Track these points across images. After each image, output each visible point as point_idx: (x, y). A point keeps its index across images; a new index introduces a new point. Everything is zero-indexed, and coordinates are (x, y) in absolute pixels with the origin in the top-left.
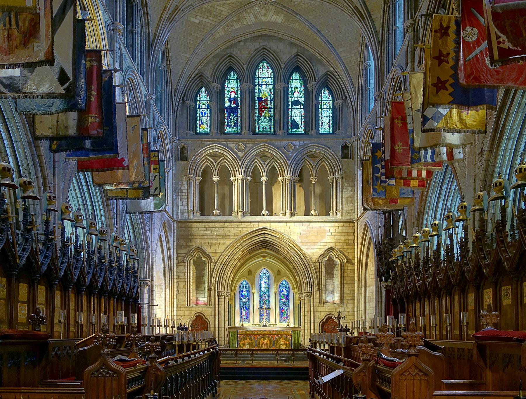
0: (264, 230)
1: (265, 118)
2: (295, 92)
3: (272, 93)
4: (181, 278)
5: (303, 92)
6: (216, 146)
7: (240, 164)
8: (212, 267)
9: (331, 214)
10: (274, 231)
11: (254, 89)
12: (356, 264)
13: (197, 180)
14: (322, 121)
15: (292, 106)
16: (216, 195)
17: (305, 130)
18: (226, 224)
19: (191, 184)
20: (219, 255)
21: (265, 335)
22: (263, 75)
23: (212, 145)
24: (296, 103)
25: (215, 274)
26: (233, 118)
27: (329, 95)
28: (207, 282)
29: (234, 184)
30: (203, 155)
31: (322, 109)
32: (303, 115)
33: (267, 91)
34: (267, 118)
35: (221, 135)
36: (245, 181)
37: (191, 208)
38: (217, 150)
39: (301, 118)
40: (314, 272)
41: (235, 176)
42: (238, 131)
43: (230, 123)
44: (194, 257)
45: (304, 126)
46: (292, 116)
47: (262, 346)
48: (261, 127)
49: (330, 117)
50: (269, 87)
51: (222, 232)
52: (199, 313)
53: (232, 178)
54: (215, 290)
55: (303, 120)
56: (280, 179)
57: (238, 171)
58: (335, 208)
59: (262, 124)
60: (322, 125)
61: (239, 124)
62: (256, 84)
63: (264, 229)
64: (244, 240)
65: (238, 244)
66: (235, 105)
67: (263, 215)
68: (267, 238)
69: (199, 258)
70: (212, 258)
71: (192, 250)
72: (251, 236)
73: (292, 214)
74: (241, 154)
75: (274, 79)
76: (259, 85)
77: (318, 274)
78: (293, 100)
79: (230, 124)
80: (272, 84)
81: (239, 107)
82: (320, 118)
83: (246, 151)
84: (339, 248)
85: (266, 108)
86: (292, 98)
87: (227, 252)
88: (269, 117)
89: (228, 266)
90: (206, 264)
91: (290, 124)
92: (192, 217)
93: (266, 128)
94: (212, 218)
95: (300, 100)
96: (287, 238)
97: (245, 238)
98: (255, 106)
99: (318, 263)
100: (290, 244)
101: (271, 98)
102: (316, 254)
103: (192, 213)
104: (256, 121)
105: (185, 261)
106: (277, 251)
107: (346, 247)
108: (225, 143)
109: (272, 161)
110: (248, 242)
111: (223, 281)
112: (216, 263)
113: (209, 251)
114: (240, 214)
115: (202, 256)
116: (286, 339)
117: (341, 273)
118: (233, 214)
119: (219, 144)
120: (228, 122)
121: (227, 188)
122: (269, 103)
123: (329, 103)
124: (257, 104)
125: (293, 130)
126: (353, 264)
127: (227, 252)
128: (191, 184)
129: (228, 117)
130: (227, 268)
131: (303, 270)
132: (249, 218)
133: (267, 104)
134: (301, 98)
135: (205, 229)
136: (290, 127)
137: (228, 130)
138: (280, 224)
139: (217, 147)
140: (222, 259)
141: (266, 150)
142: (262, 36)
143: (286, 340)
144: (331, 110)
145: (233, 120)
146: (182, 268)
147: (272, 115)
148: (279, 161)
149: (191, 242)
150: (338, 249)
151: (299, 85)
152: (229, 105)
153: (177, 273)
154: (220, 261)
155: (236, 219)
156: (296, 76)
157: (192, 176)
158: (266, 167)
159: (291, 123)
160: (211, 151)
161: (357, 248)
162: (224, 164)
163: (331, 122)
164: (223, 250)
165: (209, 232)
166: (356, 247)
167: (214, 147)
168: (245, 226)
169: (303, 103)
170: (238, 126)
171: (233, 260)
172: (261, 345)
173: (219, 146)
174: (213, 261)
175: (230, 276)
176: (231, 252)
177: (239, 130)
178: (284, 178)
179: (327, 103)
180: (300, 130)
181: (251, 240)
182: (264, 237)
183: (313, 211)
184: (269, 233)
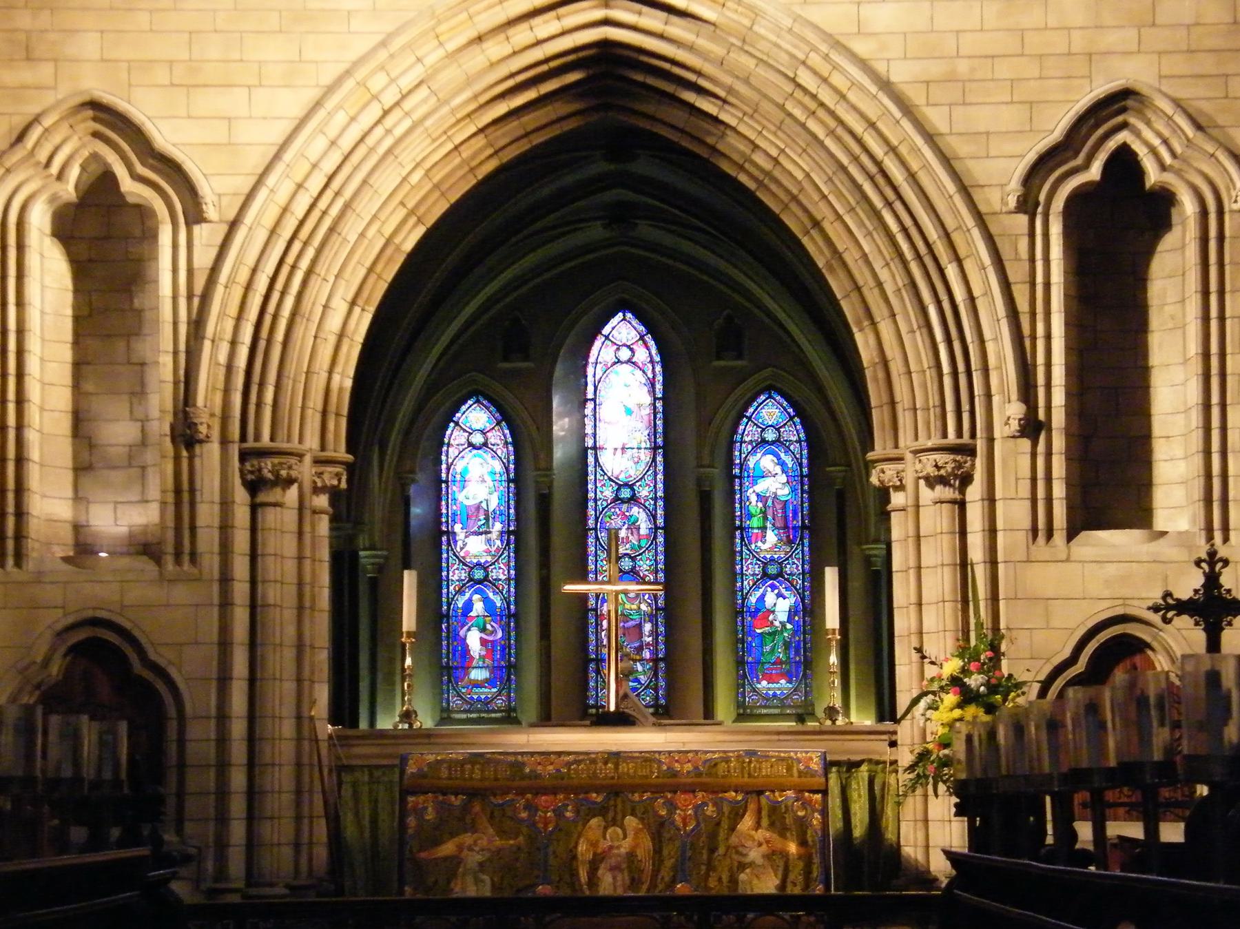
8: (203, 259)
20: (255, 161)
21: (615, 791)
40: (988, 292)
44: (60, 176)
47: (593, 880)
52: (95, 622)
54: (225, 442)
65: (406, 82)
70: (205, 189)
71: (36, 120)
77: (1023, 305)
84: (1183, 92)
87: (321, 143)
89: (328, 253)
90: (151, 236)
96: (778, 29)
100: (805, 78)
111: (291, 369)
112: (234, 225)
115: (120, 171)
116: (777, 819)
117: (1206, 293)
130: (321, 269)
140: (282, 197)
143: (783, 832)
149: (29, 57)
150: (1178, 103)
154: (262, 213)
164: (284, 128)
171: (367, 207)
172: (583, 875)
174: (211, 212)
175: (341, 336)
176: (346, 143)
182: (606, 22)
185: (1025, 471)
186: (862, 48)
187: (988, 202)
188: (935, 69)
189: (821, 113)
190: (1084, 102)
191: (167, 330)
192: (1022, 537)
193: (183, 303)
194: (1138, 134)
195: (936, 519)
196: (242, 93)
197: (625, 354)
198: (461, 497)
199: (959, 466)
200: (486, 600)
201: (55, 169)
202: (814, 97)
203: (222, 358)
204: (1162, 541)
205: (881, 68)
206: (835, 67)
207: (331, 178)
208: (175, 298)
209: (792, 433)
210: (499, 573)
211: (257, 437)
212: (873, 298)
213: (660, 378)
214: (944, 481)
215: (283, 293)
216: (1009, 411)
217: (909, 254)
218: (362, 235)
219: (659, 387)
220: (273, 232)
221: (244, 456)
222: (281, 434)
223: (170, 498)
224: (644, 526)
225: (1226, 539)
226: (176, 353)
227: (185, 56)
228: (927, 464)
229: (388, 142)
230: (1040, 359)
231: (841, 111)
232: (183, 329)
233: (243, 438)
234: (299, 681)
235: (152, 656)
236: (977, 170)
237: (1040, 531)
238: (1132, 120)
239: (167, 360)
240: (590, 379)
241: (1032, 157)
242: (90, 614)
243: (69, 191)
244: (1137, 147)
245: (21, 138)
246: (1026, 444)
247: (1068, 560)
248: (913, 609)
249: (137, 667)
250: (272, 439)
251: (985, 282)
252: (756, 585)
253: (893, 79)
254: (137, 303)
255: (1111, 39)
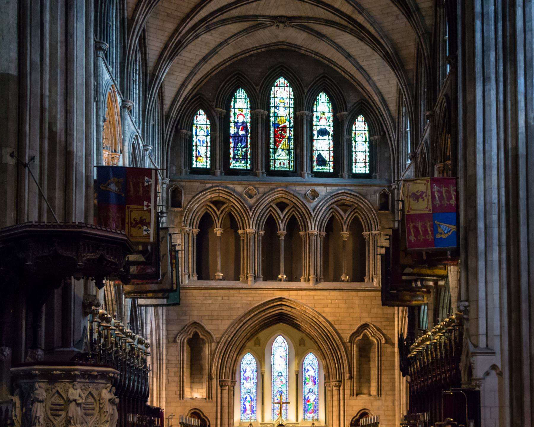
0: (281, 301)
1: (283, 150)
2: (321, 118)
3: (292, 119)
4: (173, 362)
5: (332, 119)
6: (219, 189)
7: (251, 214)
8: (213, 348)
9: (366, 280)
10: (294, 302)
11: (269, 112)
12: (396, 345)
13: (193, 233)
14: (356, 156)
15: (318, 137)
16: (219, 253)
17: (334, 168)
18: (232, 291)
19: (186, 237)
20: (222, 332)
22: (281, 94)
23: (214, 189)
24: (323, 132)
25: (216, 358)
26: (240, 149)
27: (365, 124)
28: (207, 367)
29: (242, 238)
30: (203, 201)
31: (356, 142)
32: (332, 149)
33: (285, 115)
34: (285, 151)
35: (225, 175)
36: (256, 235)
37: (186, 271)
38: (221, 195)
39: (329, 153)
41: (244, 229)
42: (247, 167)
43: (237, 155)
45: (334, 162)
46: (318, 149)
48: (277, 162)
49: (366, 152)
50: (288, 110)
51: (227, 302)
53: (240, 232)
54: (217, 379)
55: (332, 154)
56: (302, 233)
57: (247, 223)
58: (371, 273)
59: (279, 158)
60: (356, 163)
61: (249, 157)
62: (271, 105)
63: (281, 299)
64: (255, 313)
66: (243, 132)
67: (280, 280)
68: (286, 310)
69: (196, 335)
70: (214, 336)
71: (186, 325)
72: (264, 308)
73: (317, 281)
74: (251, 201)
75: (295, 100)
76: (276, 107)
77: (350, 358)
78: (319, 128)
79: (237, 157)
80: (293, 106)
81: (249, 135)
82: (354, 153)
83: (258, 196)
85: (284, 137)
86: (317, 125)
87: (233, 329)
88: (288, 150)
90: (205, 343)
91: (315, 159)
92: (187, 282)
93: (284, 164)
94: (213, 283)
95: (327, 128)
96: (310, 311)
97: (256, 311)
98: (269, 134)
99: (350, 344)
101: (291, 125)
102: (347, 332)
103: (187, 276)
104: (271, 155)
105: (177, 341)
106: (297, 327)
107: (384, 323)
108: (231, 186)
109: (292, 210)
110: (260, 316)
112: (218, 343)
113: (208, 328)
114: (250, 279)
115: (200, 334)
117: (378, 357)
118: (241, 279)
119: (223, 187)
120: (234, 155)
121: (232, 241)
122: (288, 131)
123: (365, 134)
124: (272, 132)
125: (319, 167)
126: (393, 345)
127: (233, 329)
128: (186, 237)
129: (234, 147)
130: (233, 350)
131: (330, 353)
132: (261, 284)
133: (285, 132)
134: (329, 126)
135: (204, 298)
136: (315, 164)
137: (235, 165)
138: (301, 293)
139: (220, 191)
141: (284, 196)
142: (279, 49)
144: (367, 143)
145: (240, 152)
146: (175, 349)
147: (292, 147)
148: (300, 211)
149: (185, 315)
150: (374, 326)
151: (327, 110)
152: (236, 132)
153: (166, 355)
155: (244, 286)
156: (323, 98)
157: (188, 228)
158: (284, 217)
159: (317, 158)
160: (213, 196)
161: (398, 325)
162: (229, 212)
163: (368, 159)
165: (210, 302)
166: (396, 323)
167: (217, 191)
168: (257, 295)
169: (331, 133)
170: (247, 160)
173: (223, 191)
174: (215, 340)
176: (237, 329)
177: (248, 165)
178: (307, 232)
179: (362, 133)
180: (328, 168)
181: (264, 314)
182: (281, 309)
183: (343, 275)
184: (288, 304)
185: (350, 385)
186: (323, 315)
187: (344, 341)
188: (335, 319)
189: (317, 325)
190: (359, 325)
191: (207, 360)
192: (349, 396)
193: (210, 356)
194: (368, 330)
195: (335, 393)
196: (220, 321)
197: (280, 345)
198: (245, 375)
199: (339, 384)
200: (250, 397)
201: (189, 333)
202: (316, 322)
203: (216, 365)
204: (371, 397)
205: (327, 318)
206: (319, 318)
207: (235, 334)
208: (208, 355)
209: (315, 362)
210: (253, 391)
211: (222, 378)
212: (326, 355)
213: (287, 350)
214: (337, 386)
215: (227, 354)
216: (347, 375)
217: (331, 349)
218: (239, 344)
219: (287, 352)
220: (225, 344)
221: (220, 381)
222: (226, 377)
223: (208, 388)
224: (284, 381)
225: (381, 396)
226: (208, 364)
227: (210, 314)
228: (334, 383)
229: (244, 329)
230: (352, 366)
231: (320, 325)
232: (210, 360)
233: (220, 378)
234: (229, 419)
235: (205, 414)
236: (343, 335)
237: (352, 395)
238: (367, 328)
239: (207, 365)
240: (273, 350)
241: (351, 334)
242: (194, 407)
243: (191, 336)
244: (368, 333)
245: (184, 328)
246: (350, 381)
247: (356, 399)
248: (331, 408)
249: (202, 416)
250: (225, 378)
251: (344, 354)
252: (307, 394)
253: (329, 320)
254: (201, 355)
255: (364, 315)
